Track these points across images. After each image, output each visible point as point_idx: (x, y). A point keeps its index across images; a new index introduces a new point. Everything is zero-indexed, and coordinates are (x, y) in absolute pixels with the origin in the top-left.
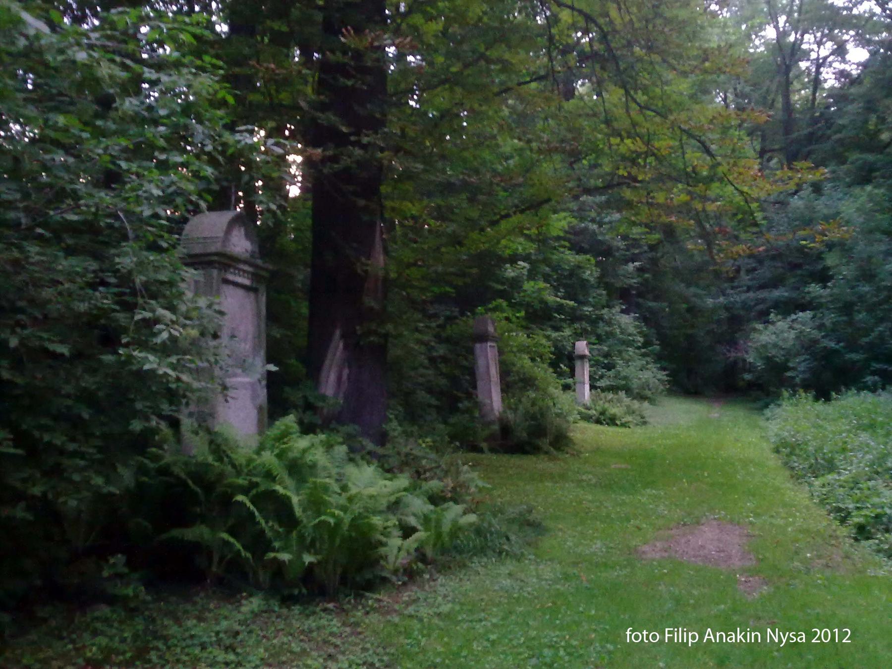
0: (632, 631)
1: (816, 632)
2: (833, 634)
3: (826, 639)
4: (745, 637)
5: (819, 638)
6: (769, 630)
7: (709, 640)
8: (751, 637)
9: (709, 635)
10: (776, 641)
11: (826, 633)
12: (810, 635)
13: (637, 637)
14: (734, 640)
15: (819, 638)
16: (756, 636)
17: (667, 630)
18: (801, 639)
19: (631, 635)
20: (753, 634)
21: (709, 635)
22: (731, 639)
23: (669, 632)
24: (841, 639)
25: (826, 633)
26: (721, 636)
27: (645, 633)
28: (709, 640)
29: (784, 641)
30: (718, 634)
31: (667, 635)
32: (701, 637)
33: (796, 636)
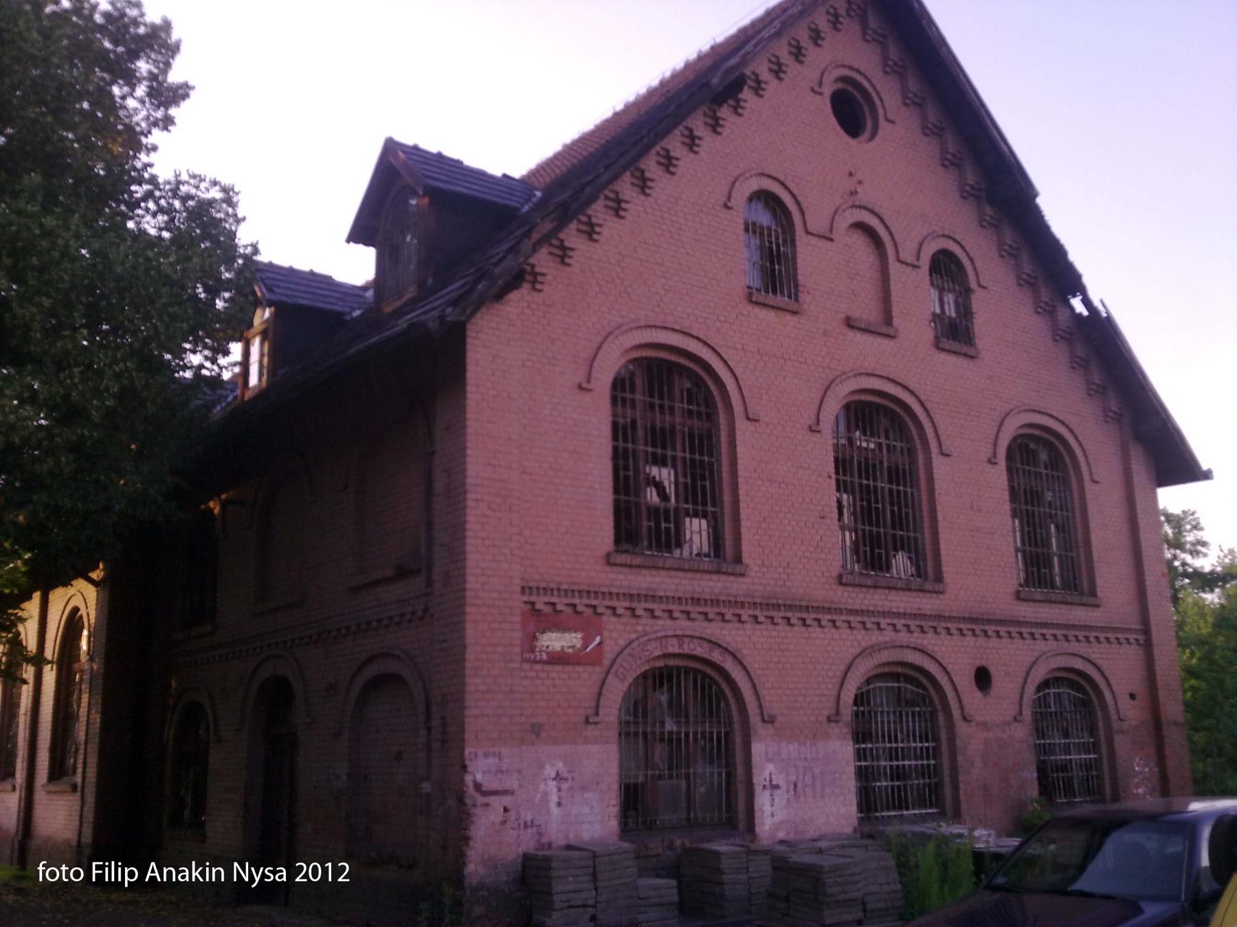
0: (46, 866)
1: (302, 867)
2: (325, 870)
3: (315, 875)
4: (203, 874)
5: (306, 876)
6: (236, 864)
7: (153, 878)
8: (214, 873)
9: (153, 871)
10: (246, 879)
11: (315, 868)
12: (293, 872)
13: (53, 874)
14: (187, 879)
15: (306, 876)
16: (218, 873)
17: (94, 864)
18: (281, 877)
19: (44, 872)
20: (214, 870)
21: (153, 871)
22: (183, 877)
23: (98, 868)
24: (335, 876)
25: (315, 868)
26: (170, 873)
27: (64, 868)
28: (153, 878)
29: (257, 879)
30: (165, 870)
31: (94, 872)
32: (143, 874)
33: (275, 873)
